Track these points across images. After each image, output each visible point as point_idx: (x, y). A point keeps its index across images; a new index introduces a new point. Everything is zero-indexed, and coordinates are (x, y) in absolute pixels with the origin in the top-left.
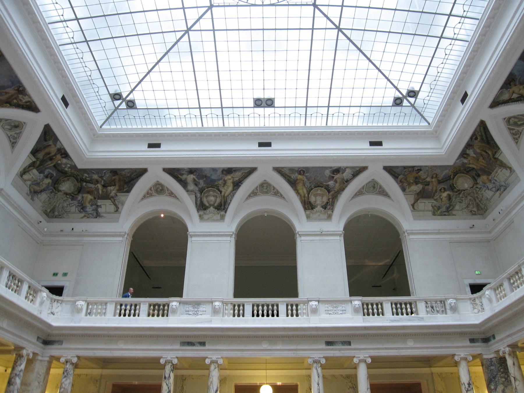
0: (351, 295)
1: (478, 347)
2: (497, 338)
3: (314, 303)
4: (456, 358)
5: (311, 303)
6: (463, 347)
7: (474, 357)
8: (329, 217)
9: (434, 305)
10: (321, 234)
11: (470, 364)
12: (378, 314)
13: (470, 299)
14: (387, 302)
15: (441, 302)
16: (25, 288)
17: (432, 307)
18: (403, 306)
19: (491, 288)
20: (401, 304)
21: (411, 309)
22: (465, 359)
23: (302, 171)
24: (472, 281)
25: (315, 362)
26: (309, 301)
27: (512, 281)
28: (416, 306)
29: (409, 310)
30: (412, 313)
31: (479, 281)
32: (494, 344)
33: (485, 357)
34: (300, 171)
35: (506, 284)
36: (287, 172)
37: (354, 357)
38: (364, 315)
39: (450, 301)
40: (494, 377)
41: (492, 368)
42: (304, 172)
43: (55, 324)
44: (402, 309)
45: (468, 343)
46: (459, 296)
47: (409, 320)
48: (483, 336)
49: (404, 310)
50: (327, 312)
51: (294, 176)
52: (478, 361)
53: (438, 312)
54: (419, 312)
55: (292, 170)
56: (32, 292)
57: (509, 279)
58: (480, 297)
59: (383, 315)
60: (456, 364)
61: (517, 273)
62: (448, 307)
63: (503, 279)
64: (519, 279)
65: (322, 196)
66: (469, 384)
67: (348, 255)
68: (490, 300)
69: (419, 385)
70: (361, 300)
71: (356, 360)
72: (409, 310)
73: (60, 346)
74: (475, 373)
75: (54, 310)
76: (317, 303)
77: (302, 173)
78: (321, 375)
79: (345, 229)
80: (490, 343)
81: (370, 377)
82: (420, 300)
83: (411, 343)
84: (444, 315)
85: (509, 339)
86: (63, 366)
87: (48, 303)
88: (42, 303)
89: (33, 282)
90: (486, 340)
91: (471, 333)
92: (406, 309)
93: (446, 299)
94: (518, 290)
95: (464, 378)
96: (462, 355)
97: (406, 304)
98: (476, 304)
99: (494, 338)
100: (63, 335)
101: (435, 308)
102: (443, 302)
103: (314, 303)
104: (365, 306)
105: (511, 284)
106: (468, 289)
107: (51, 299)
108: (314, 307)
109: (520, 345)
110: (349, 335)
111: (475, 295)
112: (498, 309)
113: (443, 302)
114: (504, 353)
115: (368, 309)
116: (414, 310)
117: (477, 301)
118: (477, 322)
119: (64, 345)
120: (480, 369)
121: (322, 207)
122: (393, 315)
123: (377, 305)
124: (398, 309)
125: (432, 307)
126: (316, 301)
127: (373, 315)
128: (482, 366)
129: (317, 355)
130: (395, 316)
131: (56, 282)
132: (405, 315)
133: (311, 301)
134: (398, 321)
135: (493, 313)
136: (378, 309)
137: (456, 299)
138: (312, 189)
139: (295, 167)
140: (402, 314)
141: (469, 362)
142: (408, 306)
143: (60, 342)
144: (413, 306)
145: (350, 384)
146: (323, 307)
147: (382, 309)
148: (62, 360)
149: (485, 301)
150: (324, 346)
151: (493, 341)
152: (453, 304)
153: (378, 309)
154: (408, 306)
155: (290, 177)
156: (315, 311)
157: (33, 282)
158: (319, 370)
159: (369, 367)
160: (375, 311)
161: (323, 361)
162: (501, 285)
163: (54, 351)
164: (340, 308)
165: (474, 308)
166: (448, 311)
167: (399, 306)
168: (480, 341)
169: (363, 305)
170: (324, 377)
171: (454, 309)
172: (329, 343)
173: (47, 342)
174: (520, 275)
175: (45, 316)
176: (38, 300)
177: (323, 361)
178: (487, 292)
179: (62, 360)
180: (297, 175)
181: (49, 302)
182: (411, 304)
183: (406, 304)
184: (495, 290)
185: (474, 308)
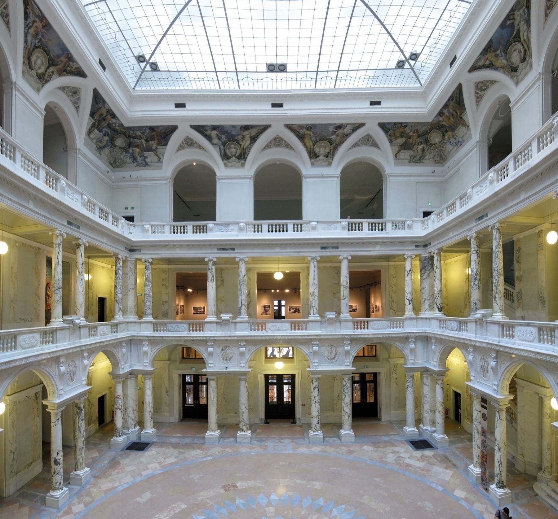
0: (341, 218)
1: (420, 250)
2: (432, 245)
3: (314, 224)
4: (405, 256)
5: (311, 223)
6: (411, 250)
7: (416, 256)
8: (330, 164)
9: (398, 225)
10: (322, 177)
11: (414, 259)
12: (359, 230)
13: (421, 221)
14: (366, 223)
15: (402, 222)
16: (110, 218)
17: (396, 226)
18: (377, 225)
19: (436, 214)
20: (375, 224)
21: (382, 227)
22: (411, 257)
23: (309, 127)
24: (425, 210)
25: (313, 259)
26: (310, 222)
27: (449, 209)
28: (385, 225)
29: (380, 227)
30: (382, 230)
31: (429, 210)
32: (430, 248)
33: (423, 256)
34: (308, 128)
35: (445, 211)
36: (297, 129)
37: (340, 256)
38: (349, 231)
39: (408, 222)
40: (425, 267)
41: (425, 262)
42: (311, 128)
43: (133, 240)
44: (375, 227)
45: (414, 248)
46: (415, 219)
47: (380, 234)
48: (424, 244)
49: (377, 228)
50: (323, 229)
51: (302, 132)
52: (418, 258)
53: (399, 228)
54: (387, 229)
55: (301, 127)
56: (115, 220)
57: (448, 208)
58: (428, 220)
59: (362, 230)
60: (405, 260)
61: (453, 204)
62: (406, 226)
63: (444, 208)
64: (454, 208)
65: (325, 147)
66: (410, 271)
67: (342, 191)
68: (433, 222)
69: (379, 272)
70: (348, 222)
71: (341, 258)
72: (380, 227)
73: (139, 253)
74: (415, 265)
75: (131, 231)
76: (316, 223)
77: (310, 129)
78: (316, 266)
79: (341, 173)
80: (427, 248)
81: (349, 267)
82: (388, 221)
83: (378, 248)
84: (403, 231)
85: (439, 245)
86: (144, 264)
87: (126, 226)
88: (123, 227)
89: (114, 214)
90: (425, 246)
91: (417, 242)
92: (379, 227)
93: (406, 221)
94: (451, 215)
95: (408, 267)
96: (409, 255)
97: (379, 224)
98: (424, 224)
99: (430, 245)
100: (140, 246)
101: (398, 226)
102: (404, 222)
103: (314, 224)
104: (350, 225)
105: (448, 211)
106: (422, 215)
107: (128, 224)
108: (314, 225)
109: (444, 249)
110: (338, 243)
111: (425, 218)
112: (436, 228)
113: (404, 222)
114: (434, 253)
115: (352, 227)
116: (384, 227)
117: (425, 222)
118: (422, 235)
119: (142, 252)
120: (418, 263)
121: (324, 156)
122: (369, 230)
123: (359, 224)
124: (372, 227)
125: (396, 226)
126: (315, 222)
127: (355, 230)
128: (420, 261)
129: (314, 255)
130: (370, 231)
131: (129, 213)
132: (377, 230)
133: (312, 222)
134: (372, 234)
135: (434, 229)
136: (359, 227)
137: (413, 221)
138: (317, 142)
139: (304, 124)
140: (375, 230)
141: (412, 258)
142: (380, 225)
143: (140, 250)
144: (383, 225)
145: (336, 271)
146: (320, 226)
147: (362, 227)
148: (143, 260)
149: (430, 222)
150: (319, 250)
151: (429, 246)
152: (410, 224)
153: (359, 227)
154: (380, 225)
155: (299, 133)
156: (314, 228)
157: (114, 214)
158: (316, 263)
159: (349, 261)
160: (357, 228)
161: (319, 258)
162: (442, 212)
163: (137, 255)
164: (332, 226)
165: (422, 227)
166: (406, 228)
167: (374, 225)
168: (422, 246)
169: (349, 224)
170: (318, 268)
171: (410, 227)
172: (323, 248)
173: (131, 251)
174: (454, 206)
175: (126, 235)
176: (120, 225)
177: (319, 258)
178: (433, 216)
179: (143, 260)
180: (305, 130)
181: (127, 226)
182: (382, 224)
183: (379, 224)
184: (438, 215)
185: (422, 227)
